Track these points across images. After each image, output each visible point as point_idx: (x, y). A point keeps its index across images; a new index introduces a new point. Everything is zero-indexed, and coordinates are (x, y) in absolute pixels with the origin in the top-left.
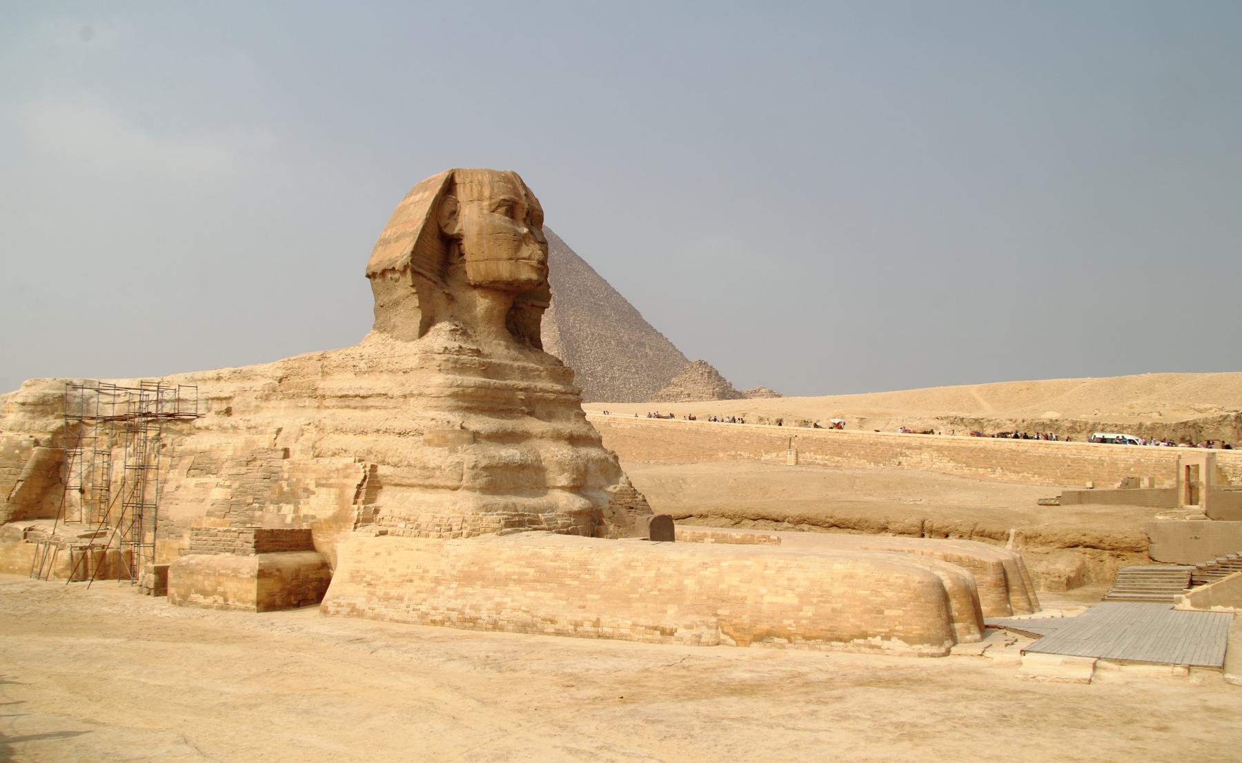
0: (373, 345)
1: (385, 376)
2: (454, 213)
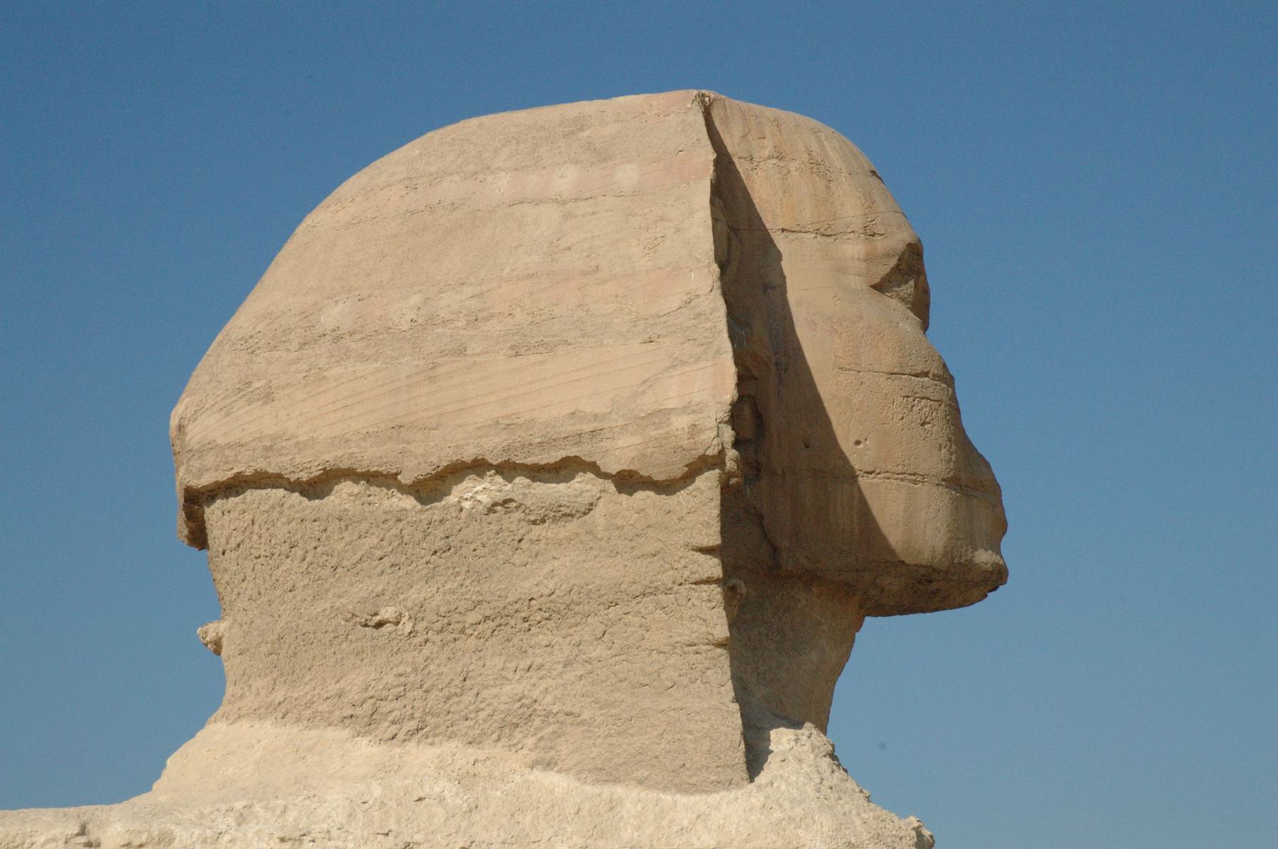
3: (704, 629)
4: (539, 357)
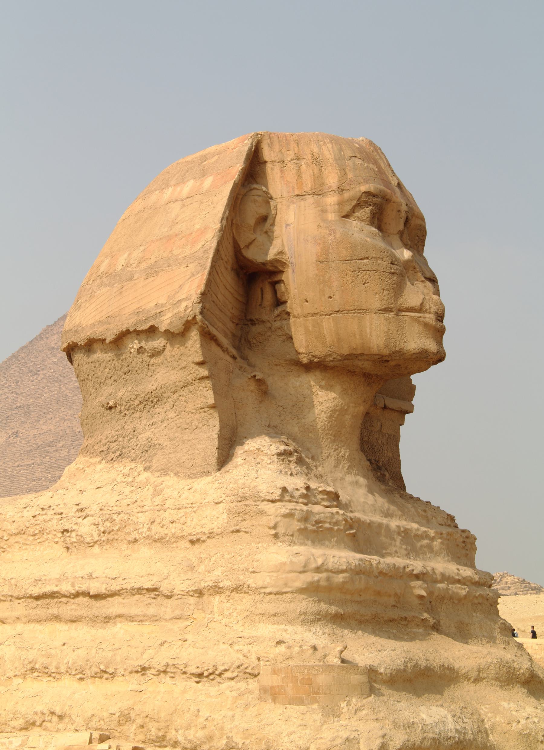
0: (91, 485)
1: (145, 552)
2: (264, 220)
3: (205, 401)
4: (153, 278)
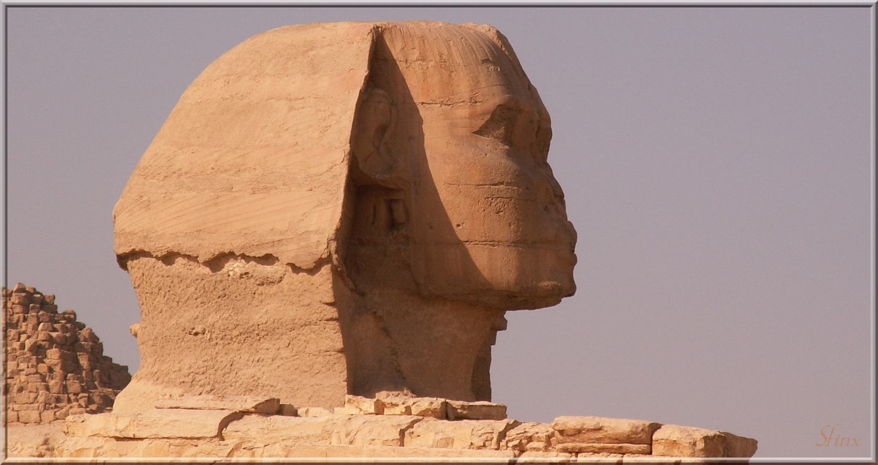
4: (262, 195)
